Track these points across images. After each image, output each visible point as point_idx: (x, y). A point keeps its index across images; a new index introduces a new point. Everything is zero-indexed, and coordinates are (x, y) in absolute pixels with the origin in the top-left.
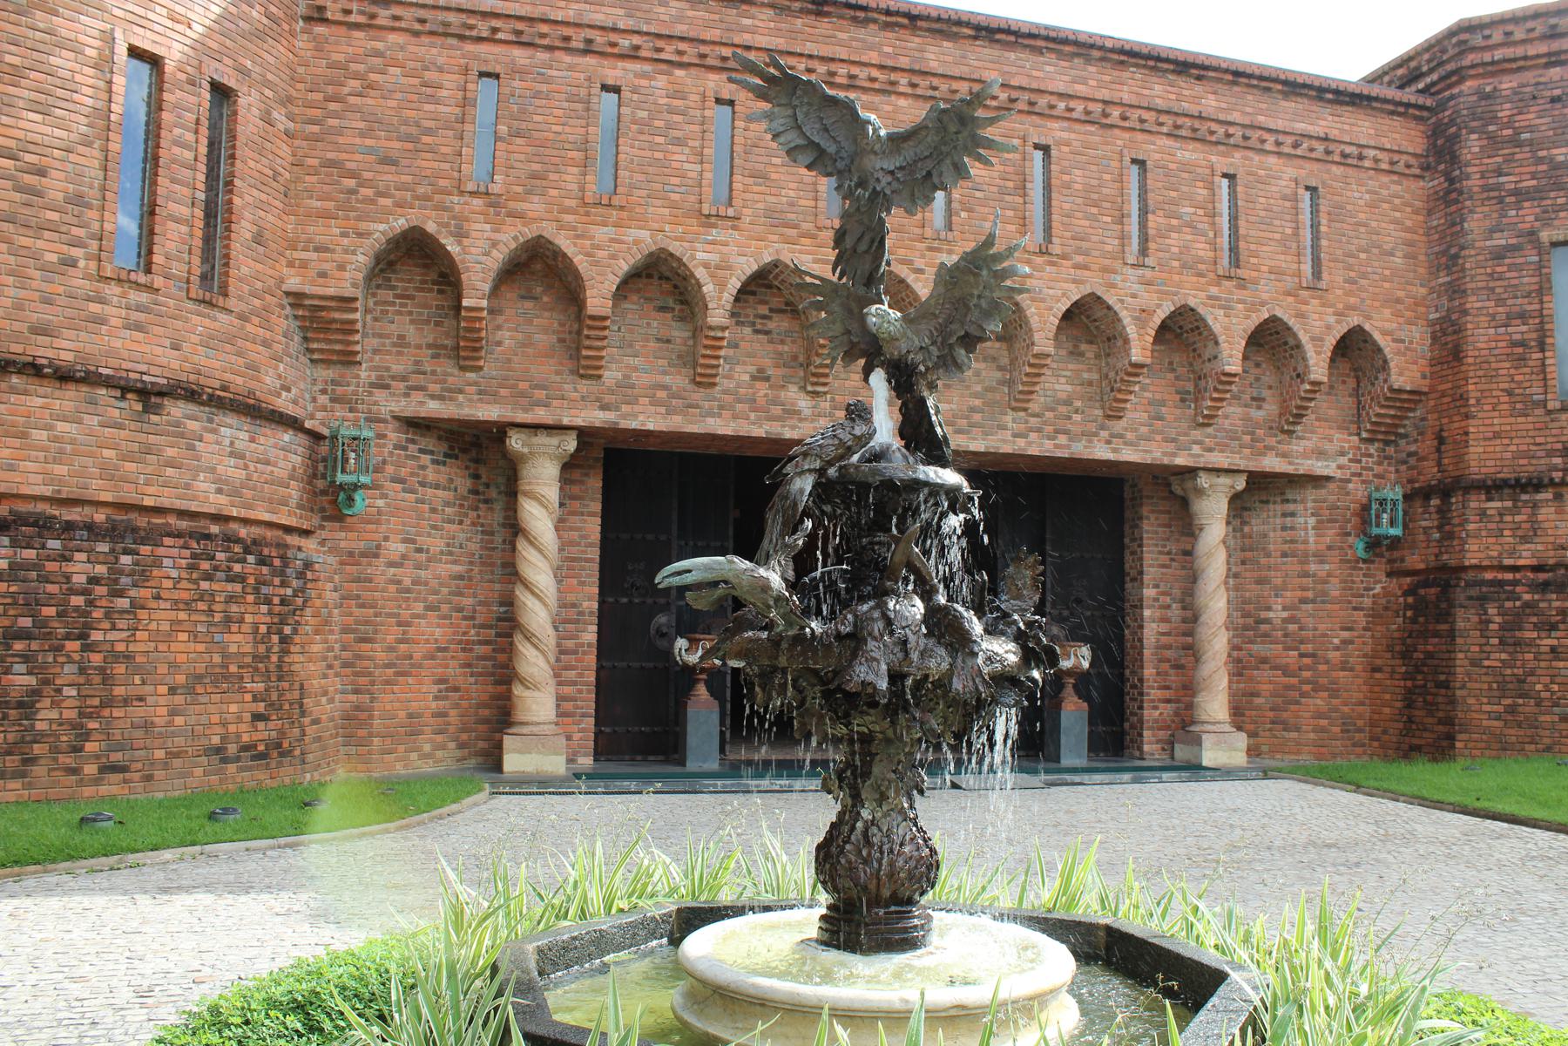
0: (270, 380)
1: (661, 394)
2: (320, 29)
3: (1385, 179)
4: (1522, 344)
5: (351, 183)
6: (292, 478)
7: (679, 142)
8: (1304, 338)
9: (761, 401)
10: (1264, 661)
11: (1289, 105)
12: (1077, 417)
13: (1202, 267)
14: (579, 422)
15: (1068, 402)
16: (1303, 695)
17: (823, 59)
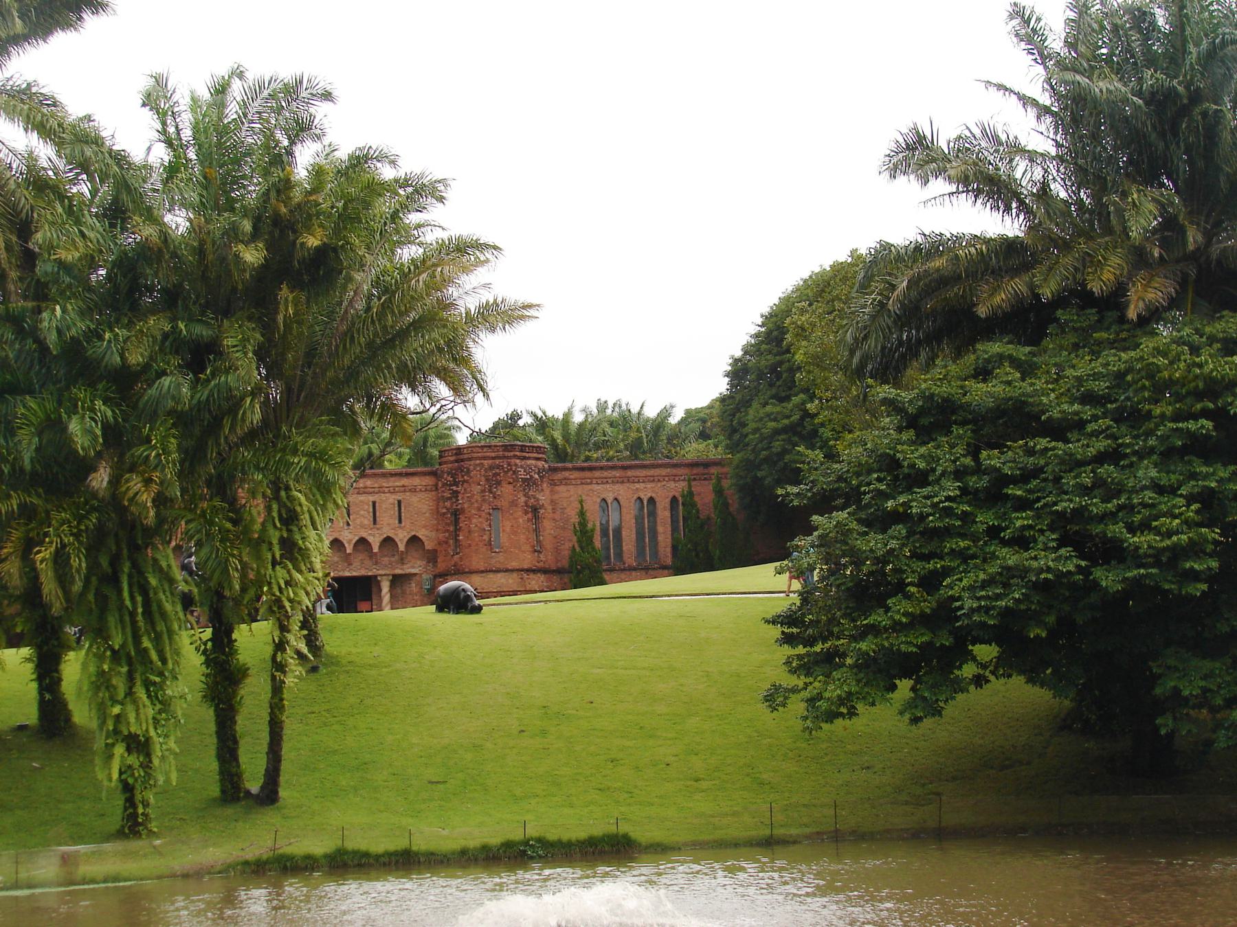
11: (393, 479)
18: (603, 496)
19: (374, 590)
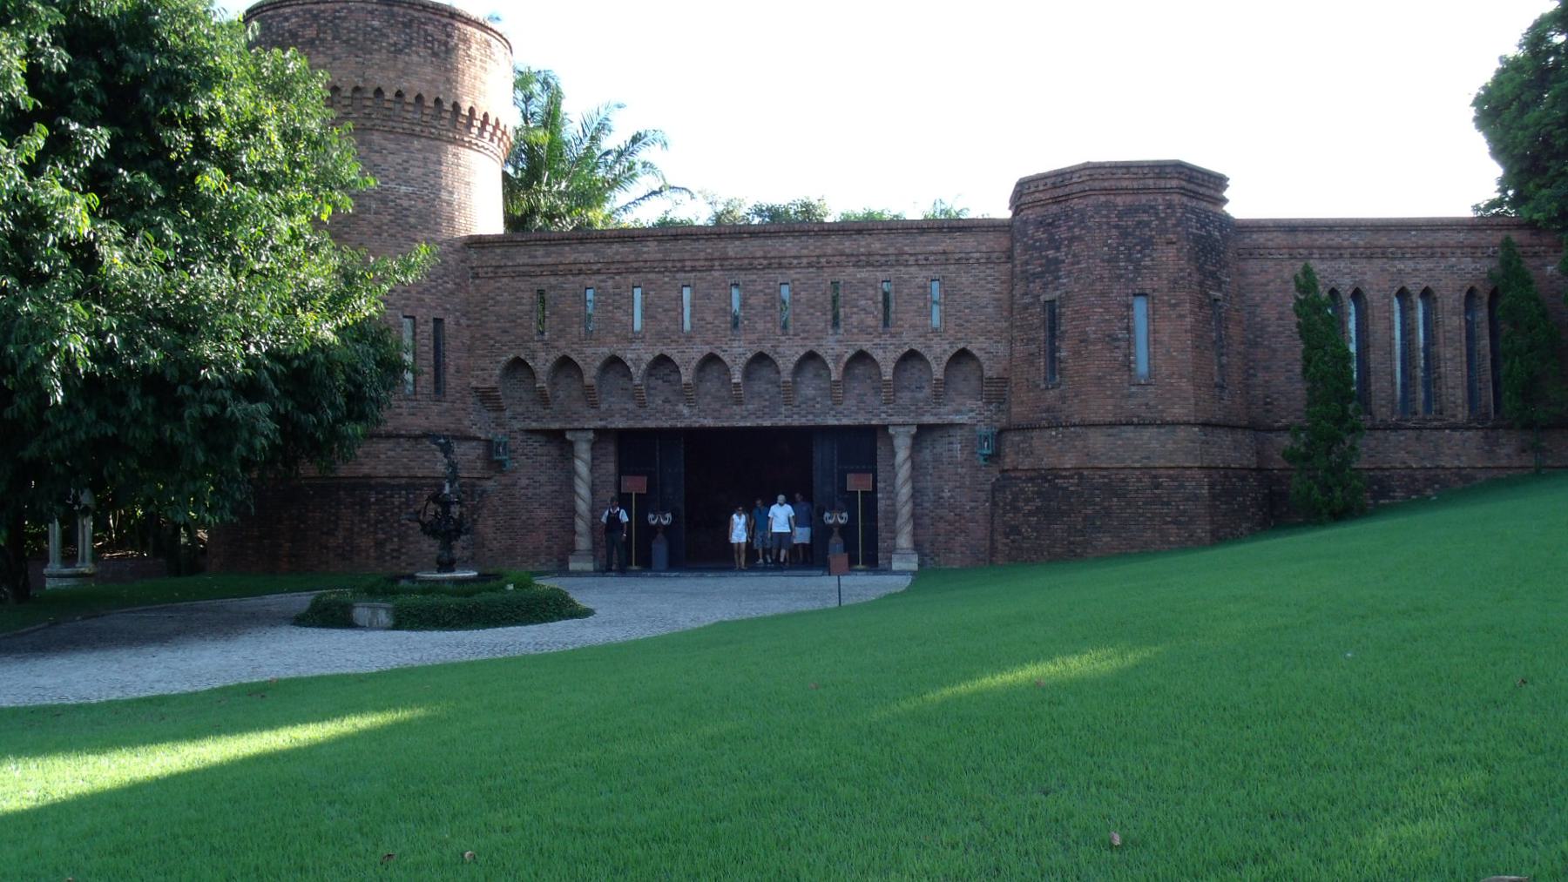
0: (466, 423)
1: (625, 412)
2: (477, 281)
3: (983, 268)
4: (1032, 354)
5: (492, 342)
6: (478, 458)
7: (619, 308)
8: (929, 358)
9: (667, 411)
10: (941, 518)
11: (924, 238)
12: (818, 406)
13: (870, 330)
14: (591, 427)
15: (814, 399)
16: (956, 535)
17: (679, 261)
18: (1333, 284)
19: (881, 451)
